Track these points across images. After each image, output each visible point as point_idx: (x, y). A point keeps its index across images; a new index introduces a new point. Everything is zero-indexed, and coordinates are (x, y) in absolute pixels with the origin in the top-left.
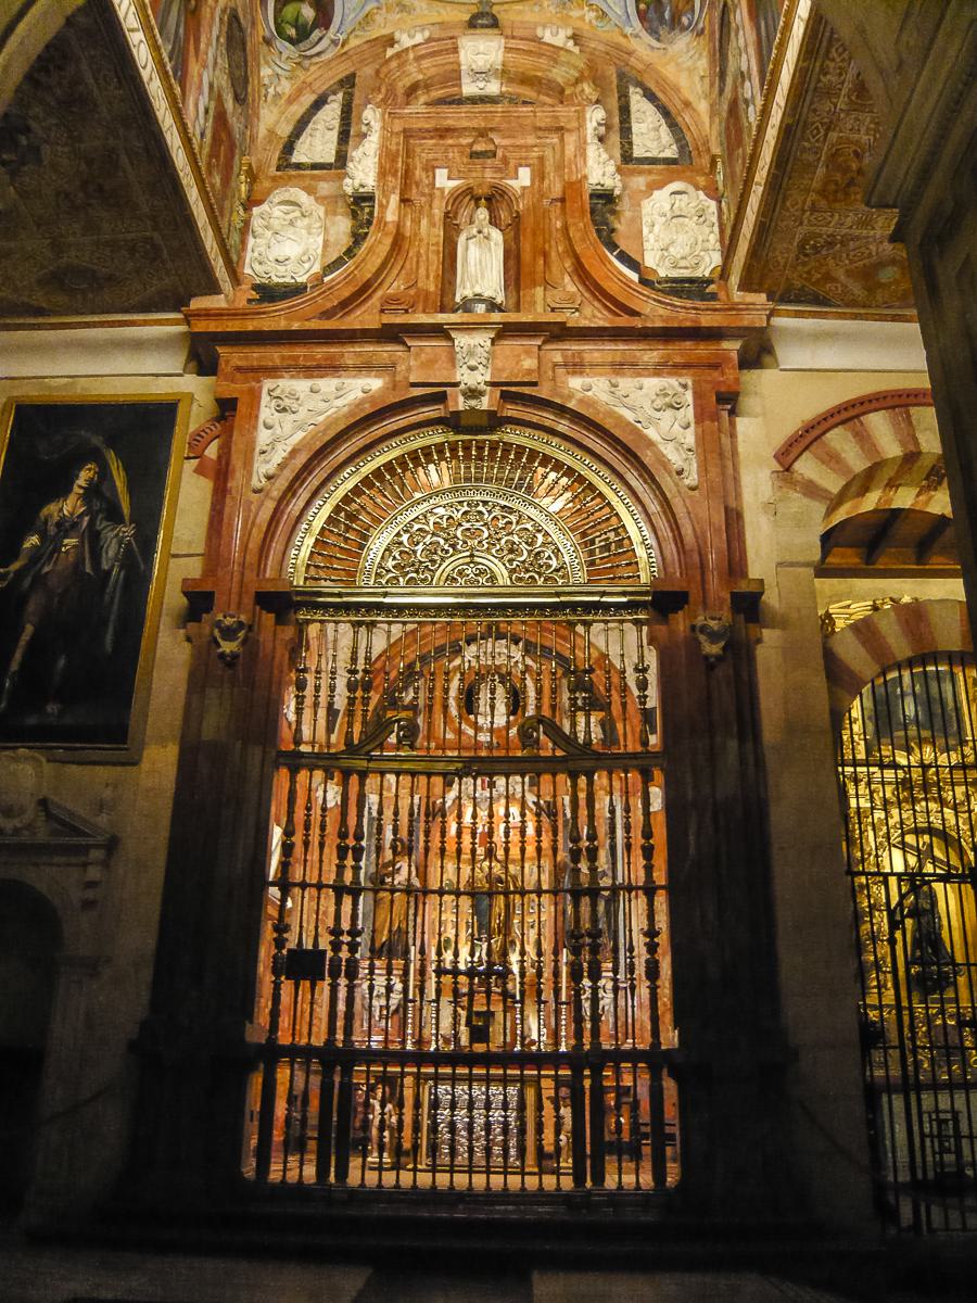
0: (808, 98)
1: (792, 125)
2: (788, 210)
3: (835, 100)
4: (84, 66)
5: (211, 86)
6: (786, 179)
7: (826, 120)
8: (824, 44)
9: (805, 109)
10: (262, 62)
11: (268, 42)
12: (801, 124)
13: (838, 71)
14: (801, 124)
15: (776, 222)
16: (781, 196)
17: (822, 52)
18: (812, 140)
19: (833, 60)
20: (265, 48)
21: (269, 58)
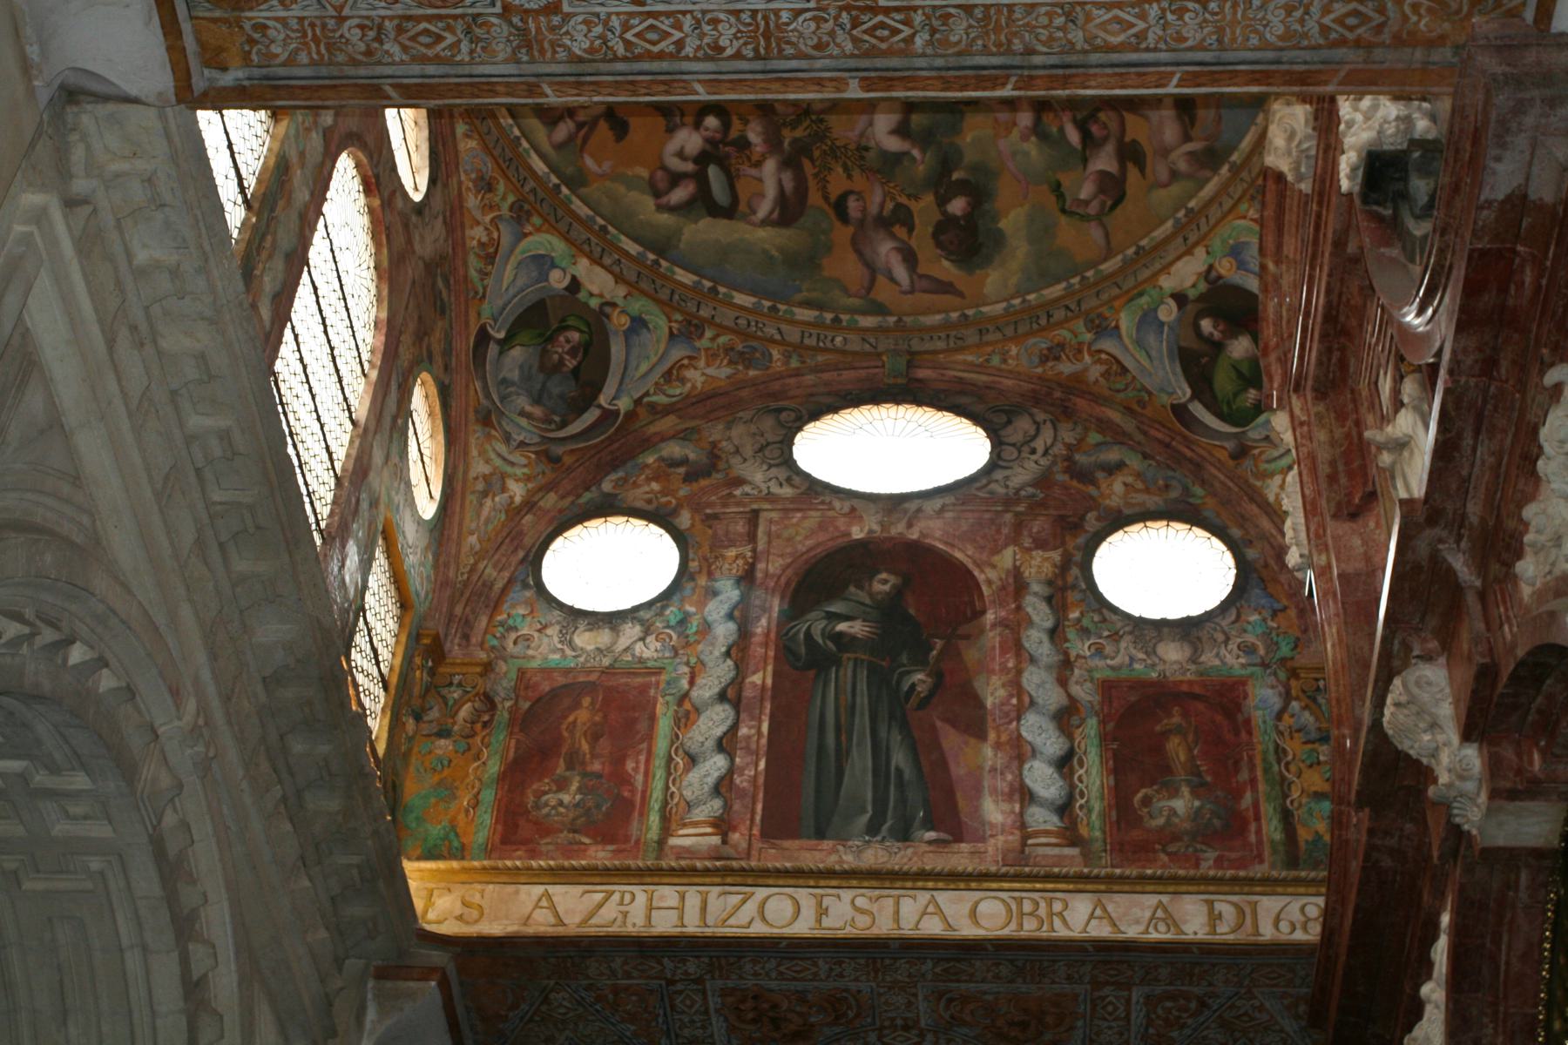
0: (794, 64)
1: (863, 79)
2: (1141, 36)
3: (785, 17)
4: (773, 985)
5: (1065, 718)
6: (1037, 60)
7: (845, 18)
8: (646, 66)
9: (819, 64)
10: (1258, 484)
11: (1241, 452)
12: (866, 63)
13: (706, 28)
14: (866, 63)
15: (1190, 49)
16: (1095, 58)
17: (665, 65)
18: (907, 31)
19: (680, 44)
20: (1248, 463)
21: (1263, 466)
